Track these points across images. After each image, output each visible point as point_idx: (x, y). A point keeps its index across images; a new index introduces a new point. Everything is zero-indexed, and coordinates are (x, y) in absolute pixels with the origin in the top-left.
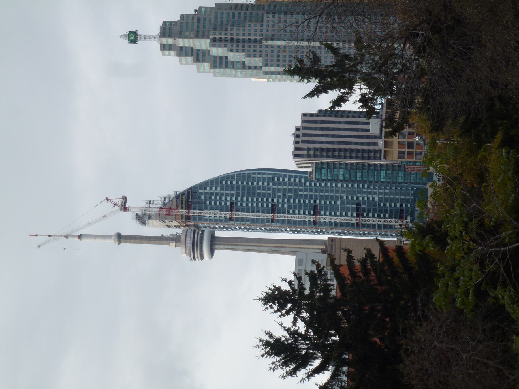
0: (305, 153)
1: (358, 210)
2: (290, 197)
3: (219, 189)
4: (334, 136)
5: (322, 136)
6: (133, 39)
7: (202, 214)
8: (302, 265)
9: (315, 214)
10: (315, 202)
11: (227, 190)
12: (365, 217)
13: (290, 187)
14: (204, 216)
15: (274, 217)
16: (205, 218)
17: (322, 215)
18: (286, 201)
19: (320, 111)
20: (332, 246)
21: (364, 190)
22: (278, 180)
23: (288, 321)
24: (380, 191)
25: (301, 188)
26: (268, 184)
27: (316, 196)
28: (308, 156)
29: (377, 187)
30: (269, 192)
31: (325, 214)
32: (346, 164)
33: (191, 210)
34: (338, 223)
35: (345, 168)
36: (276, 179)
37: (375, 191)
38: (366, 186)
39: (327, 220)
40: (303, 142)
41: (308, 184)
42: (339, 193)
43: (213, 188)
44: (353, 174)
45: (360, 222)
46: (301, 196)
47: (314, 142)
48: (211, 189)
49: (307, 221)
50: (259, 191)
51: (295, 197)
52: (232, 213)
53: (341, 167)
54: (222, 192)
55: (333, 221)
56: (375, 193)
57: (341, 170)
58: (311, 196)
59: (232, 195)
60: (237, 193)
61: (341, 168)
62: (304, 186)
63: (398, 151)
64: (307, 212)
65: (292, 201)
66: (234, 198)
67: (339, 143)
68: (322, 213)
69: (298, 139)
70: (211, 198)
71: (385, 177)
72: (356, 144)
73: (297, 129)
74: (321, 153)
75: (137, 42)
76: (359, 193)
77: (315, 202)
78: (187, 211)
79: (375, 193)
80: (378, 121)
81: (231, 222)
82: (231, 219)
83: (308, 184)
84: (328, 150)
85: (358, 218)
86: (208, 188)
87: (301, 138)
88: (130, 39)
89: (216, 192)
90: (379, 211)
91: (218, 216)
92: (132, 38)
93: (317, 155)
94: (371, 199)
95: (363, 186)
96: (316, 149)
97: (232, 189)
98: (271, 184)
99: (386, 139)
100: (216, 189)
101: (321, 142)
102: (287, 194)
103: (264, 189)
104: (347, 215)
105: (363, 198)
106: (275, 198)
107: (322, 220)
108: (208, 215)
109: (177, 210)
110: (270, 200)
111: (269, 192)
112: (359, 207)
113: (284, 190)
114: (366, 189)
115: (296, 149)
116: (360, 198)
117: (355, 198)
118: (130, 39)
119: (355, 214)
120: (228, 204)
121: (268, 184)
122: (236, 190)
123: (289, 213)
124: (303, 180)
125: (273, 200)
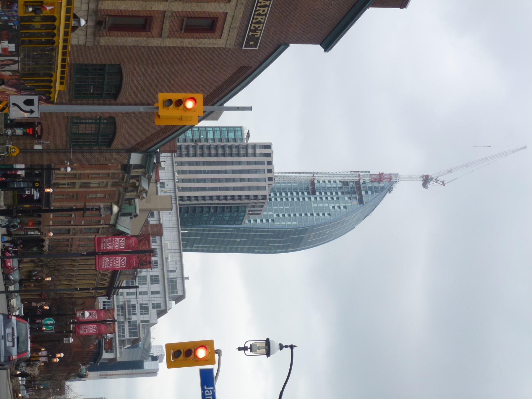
4: (226, 172)
5: (240, 172)
22: (267, 221)
26: (278, 215)
36: (270, 221)
40: (262, 163)
47: (249, 163)
48: (339, 207)
50: (287, 207)
54: (327, 205)
60: (312, 205)
66: (313, 199)
69: (269, 167)
70: (338, 198)
72: (197, 164)
89: (333, 205)
93: (243, 148)
96: (247, 155)
98: (275, 215)
100: (334, 207)
101: (240, 163)
103: (281, 210)
115: (269, 155)
120: (317, 193)
121: (278, 215)
122: (312, 208)
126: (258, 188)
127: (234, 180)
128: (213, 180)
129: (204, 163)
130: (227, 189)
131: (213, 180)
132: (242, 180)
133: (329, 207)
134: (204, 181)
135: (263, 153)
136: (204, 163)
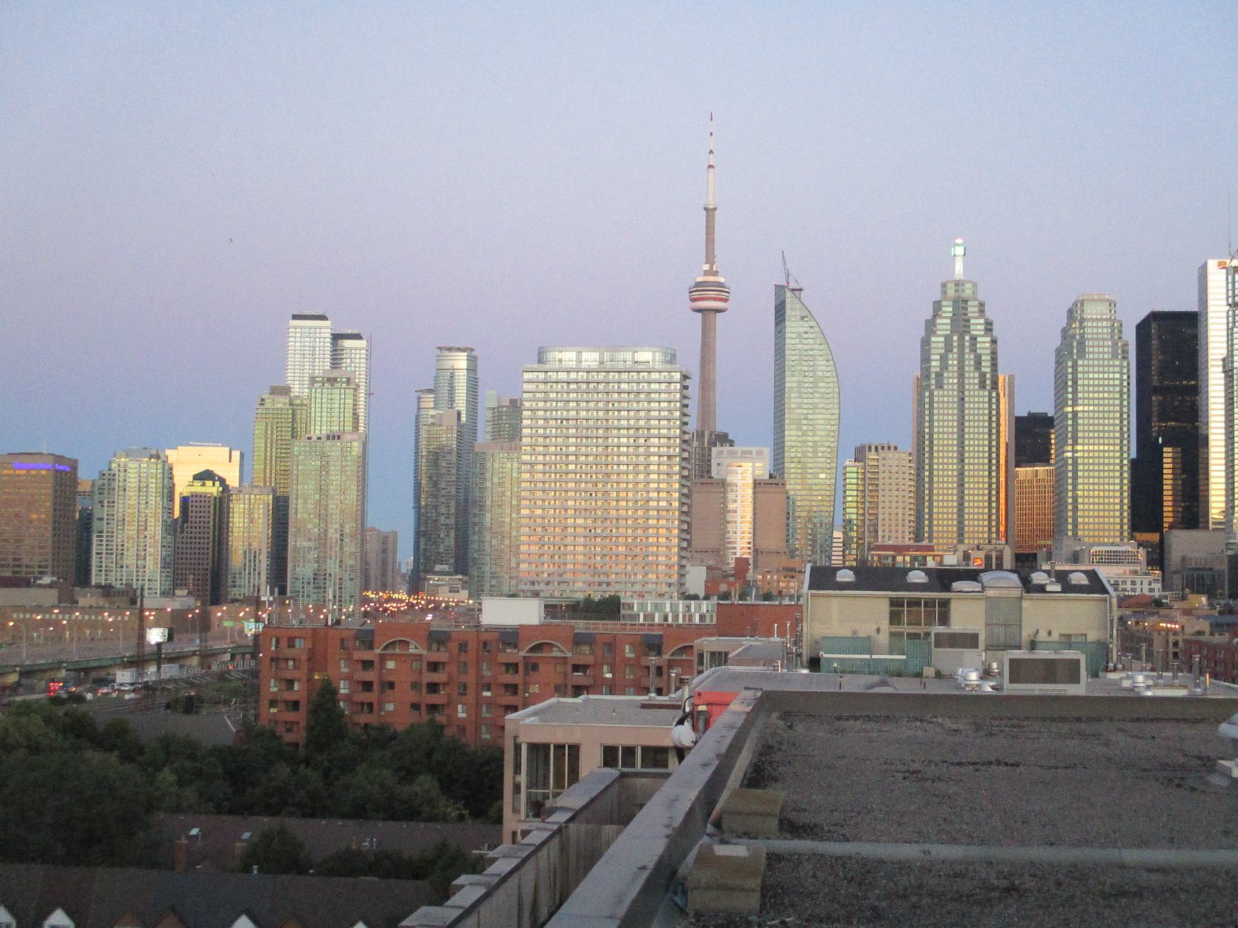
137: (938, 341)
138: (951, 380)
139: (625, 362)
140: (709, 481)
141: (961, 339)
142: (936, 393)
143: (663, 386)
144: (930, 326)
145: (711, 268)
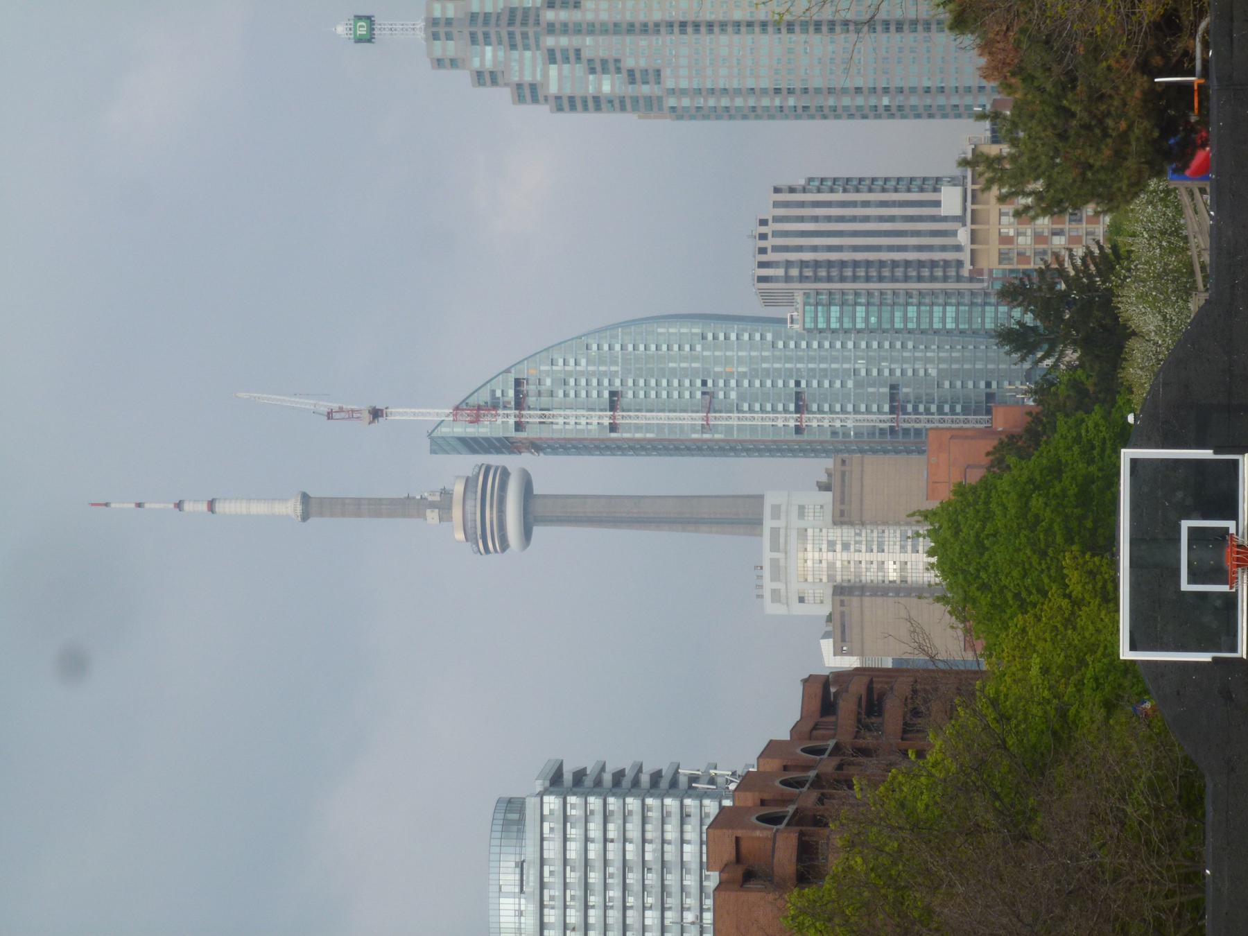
0: (780, 272)
1: (893, 398)
2: (744, 375)
3: (583, 362)
6: (365, 33)
7: (549, 418)
8: (779, 518)
9: (798, 409)
10: (798, 384)
11: (601, 362)
12: (909, 414)
13: (740, 354)
14: (552, 423)
15: (707, 420)
16: (555, 427)
17: (814, 413)
18: (733, 383)
19: (810, 180)
20: (843, 473)
21: (905, 354)
22: (715, 337)
23: (1017, 313)
24: (941, 354)
25: (765, 354)
27: (798, 370)
28: (787, 279)
29: (934, 347)
30: (694, 365)
31: (820, 411)
32: (869, 294)
33: (524, 409)
34: (850, 429)
35: (868, 304)
36: (710, 336)
37: (929, 354)
38: (910, 345)
39: (826, 424)
40: (776, 249)
41: (780, 344)
42: (850, 363)
43: (572, 362)
44: (886, 315)
45: (898, 426)
46: (767, 373)
47: (799, 249)
49: (780, 428)
51: (753, 374)
52: (616, 414)
53: (859, 300)
54: (591, 368)
55: (838, 424)
56: (927, 360)
57: (859, 308)
58: (790, 370)
59: (615, 374)
61: (860, 304)
62: (771, 349)
63: (999, 250)
64: (780, 407)
65: (746, 383)
66: (617, 382)
67: (856, 249)
68: (815, 407)
69: (763, 244)
70: (565, 383)
71: (956, 320)
73: (763, 222)
74: (815, 272)
75: (373, 40)
76: (892, 360)
77: (798, 384)
78: (517, 412)
79: (927, 360)
80: (958, 191)
81: (613, 435)
82: (613, 428)
83: (780, 344)
84: (830, 264)
85: (895, 416)
86: (561, 362)
87: (771, 242)
88: (359, 32)
90: (939, 399)
91: (583, 421)
92: (362, 31)
94: (922, 373)
95: (903, 346)
96: (803, 264)
97: (615, 363)
98: (699, 348)
99: (974, 227)
101: (815, 249)
102: (735, 370)
103: (684, 359)
104: (868, 411)
105: (903, 372)
106: (710, 377)
107: (815, 424)
108: (561, 421)
109: (494, 412)
110: (698, 383)
111: (694, 365)
112: (895, 391)
113: (728, 361)
114: (910, 351)
116: (898, 373)
117: (886, 373)
118: (359, 32)
119: (886, 408)
120: (606, 394)
123: (739, 411)
124: (769, 337)
125: (704, 383)
126: (786, 204)
127: (829, 219)
128: (866, 219)
129: (878, 248)
130: (843, 204)
131: (866, 219)
132: (816, 219)
133: (587, 365)
134: (881, 219)
135: (772, 268)
136: (878, 248)
137: (555, 79)
138: (637, 51)
139: (521, 914)
140: (837, 617)
141: (551, 29)
142: (670, 84)
143: (573, 832)
144: (529, 93)
145: (433, 505)
